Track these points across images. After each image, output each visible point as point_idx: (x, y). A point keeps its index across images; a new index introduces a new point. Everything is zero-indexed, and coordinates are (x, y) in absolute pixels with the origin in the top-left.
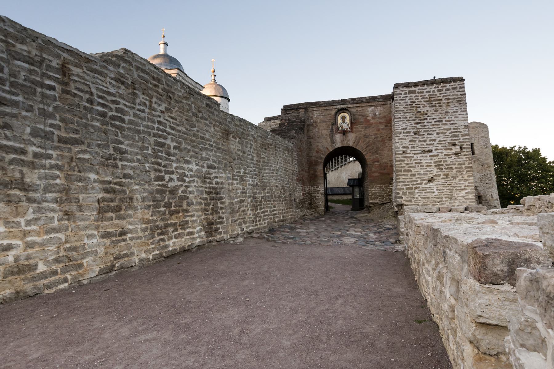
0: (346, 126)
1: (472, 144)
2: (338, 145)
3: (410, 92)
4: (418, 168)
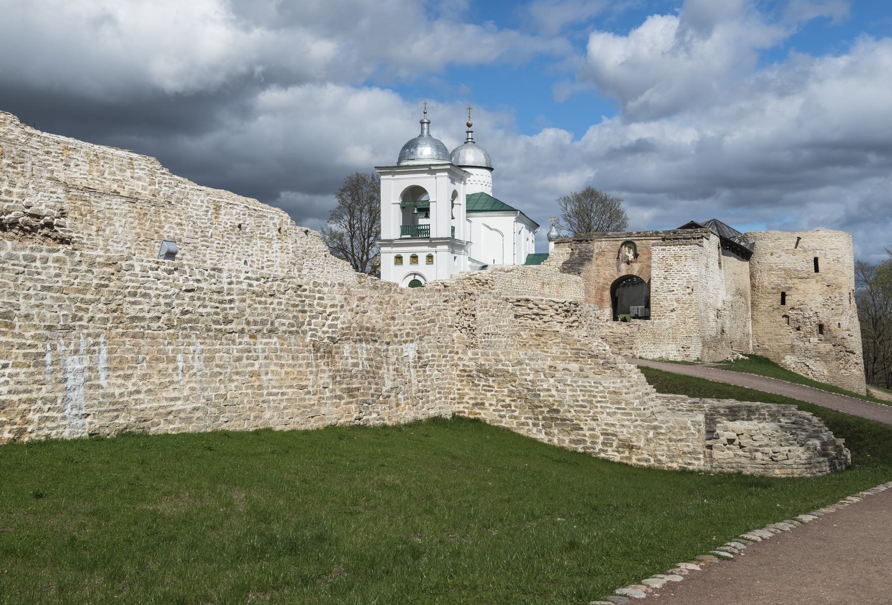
0: (631, 256)
1: (816, 260)
2: (623, 273)
3: (662, 250)
4: (665, 301)
